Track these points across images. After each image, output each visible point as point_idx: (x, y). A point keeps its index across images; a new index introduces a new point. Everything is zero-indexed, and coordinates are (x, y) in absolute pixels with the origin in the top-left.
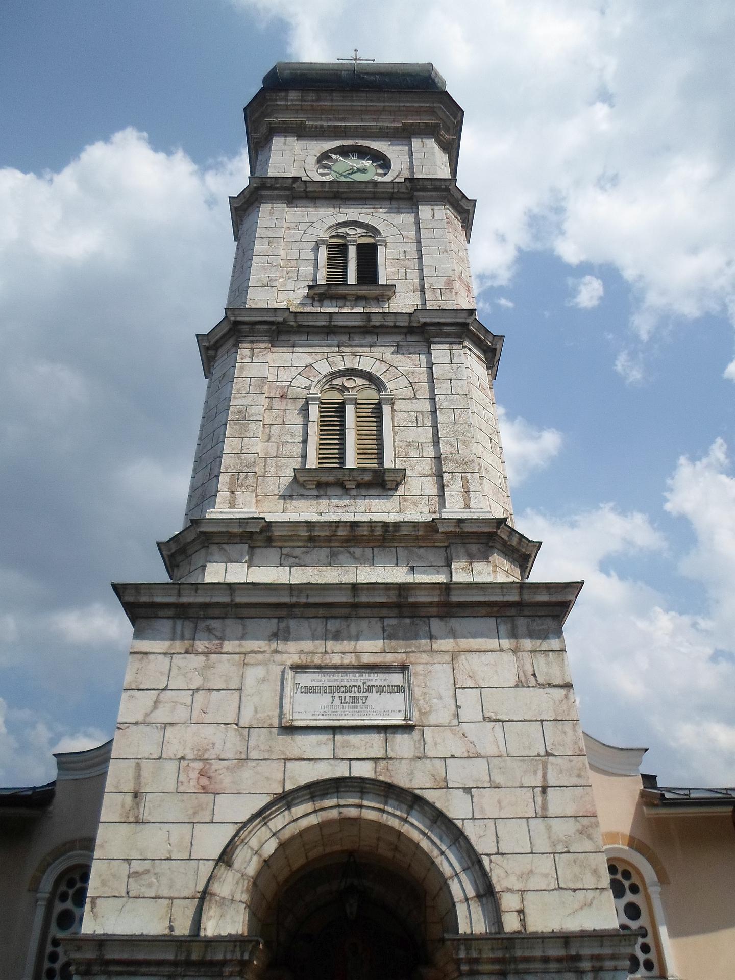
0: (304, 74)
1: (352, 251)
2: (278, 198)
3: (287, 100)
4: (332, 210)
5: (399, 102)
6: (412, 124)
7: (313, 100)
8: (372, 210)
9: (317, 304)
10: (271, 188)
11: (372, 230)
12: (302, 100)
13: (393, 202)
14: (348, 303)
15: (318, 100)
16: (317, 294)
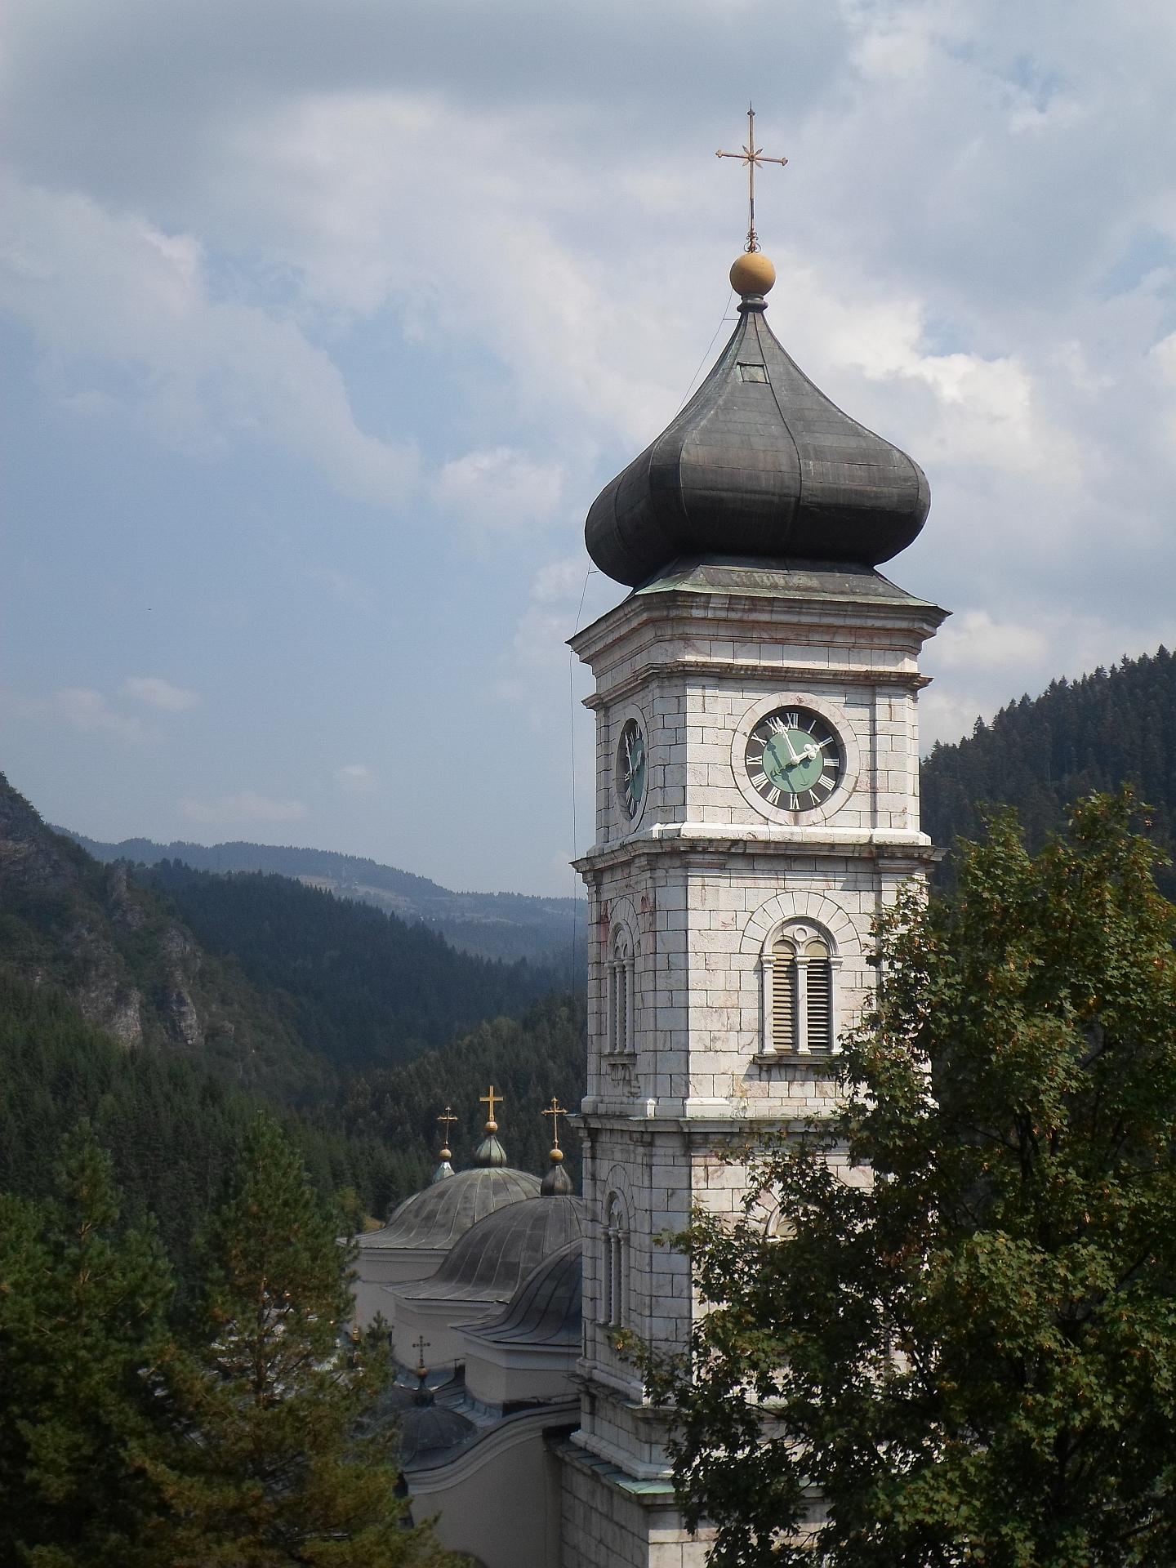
0: (721, 500)
1: (802, 976)
2: (710, 866)
3: (706, 608)
4: (774, 883)
5: (867, 617)
6: (881, 674)
7: (744, 610)
8: (823, 885)
9: (764, 1075)
10: (705, 851)
11: (826, 937)
12: (728, 609)
13: (851, 868)
14: (798, 1074)
15: (750, 610)
16: (765, 1067)
